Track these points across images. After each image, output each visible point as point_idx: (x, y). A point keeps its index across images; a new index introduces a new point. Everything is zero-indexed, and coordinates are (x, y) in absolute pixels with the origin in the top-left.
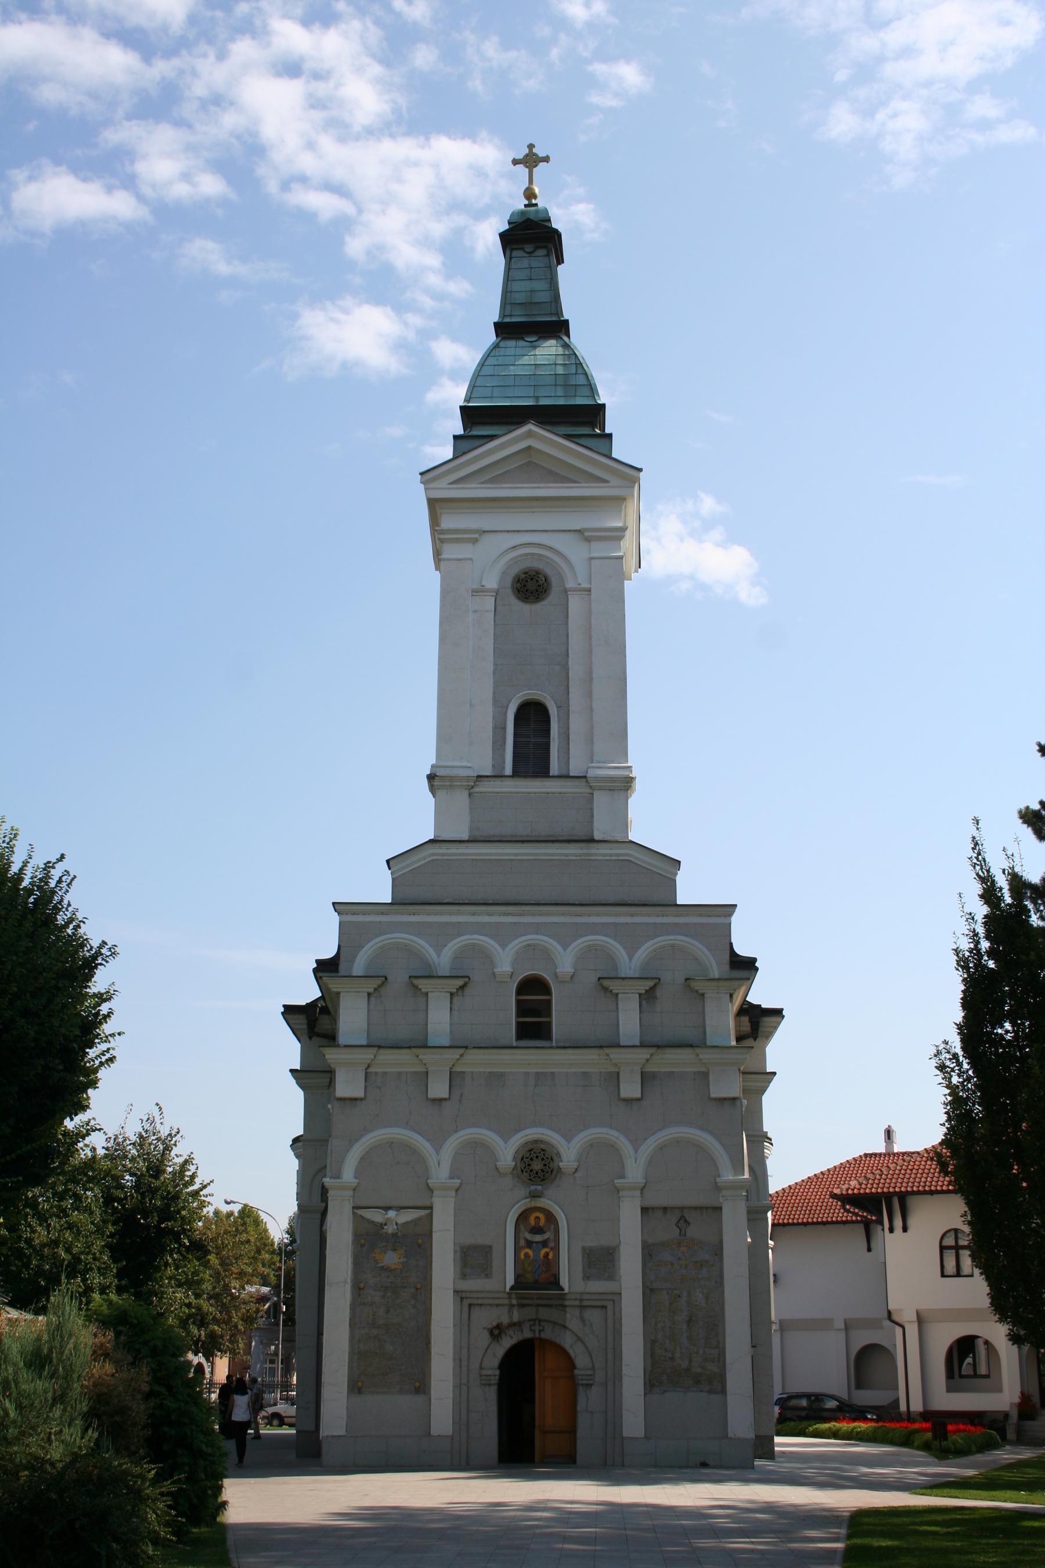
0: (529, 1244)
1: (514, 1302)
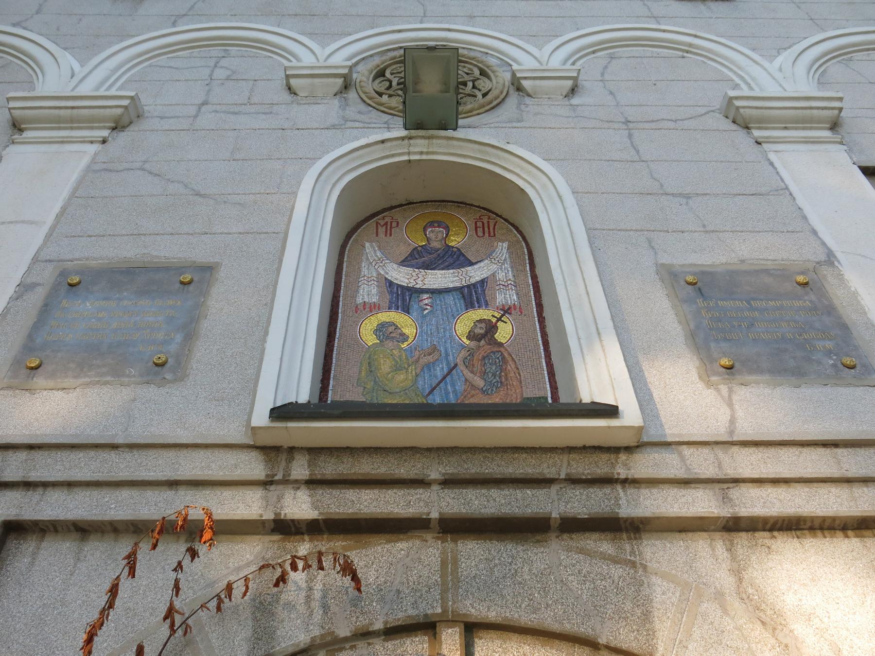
0: (402, 298)
1: (299, 506)
